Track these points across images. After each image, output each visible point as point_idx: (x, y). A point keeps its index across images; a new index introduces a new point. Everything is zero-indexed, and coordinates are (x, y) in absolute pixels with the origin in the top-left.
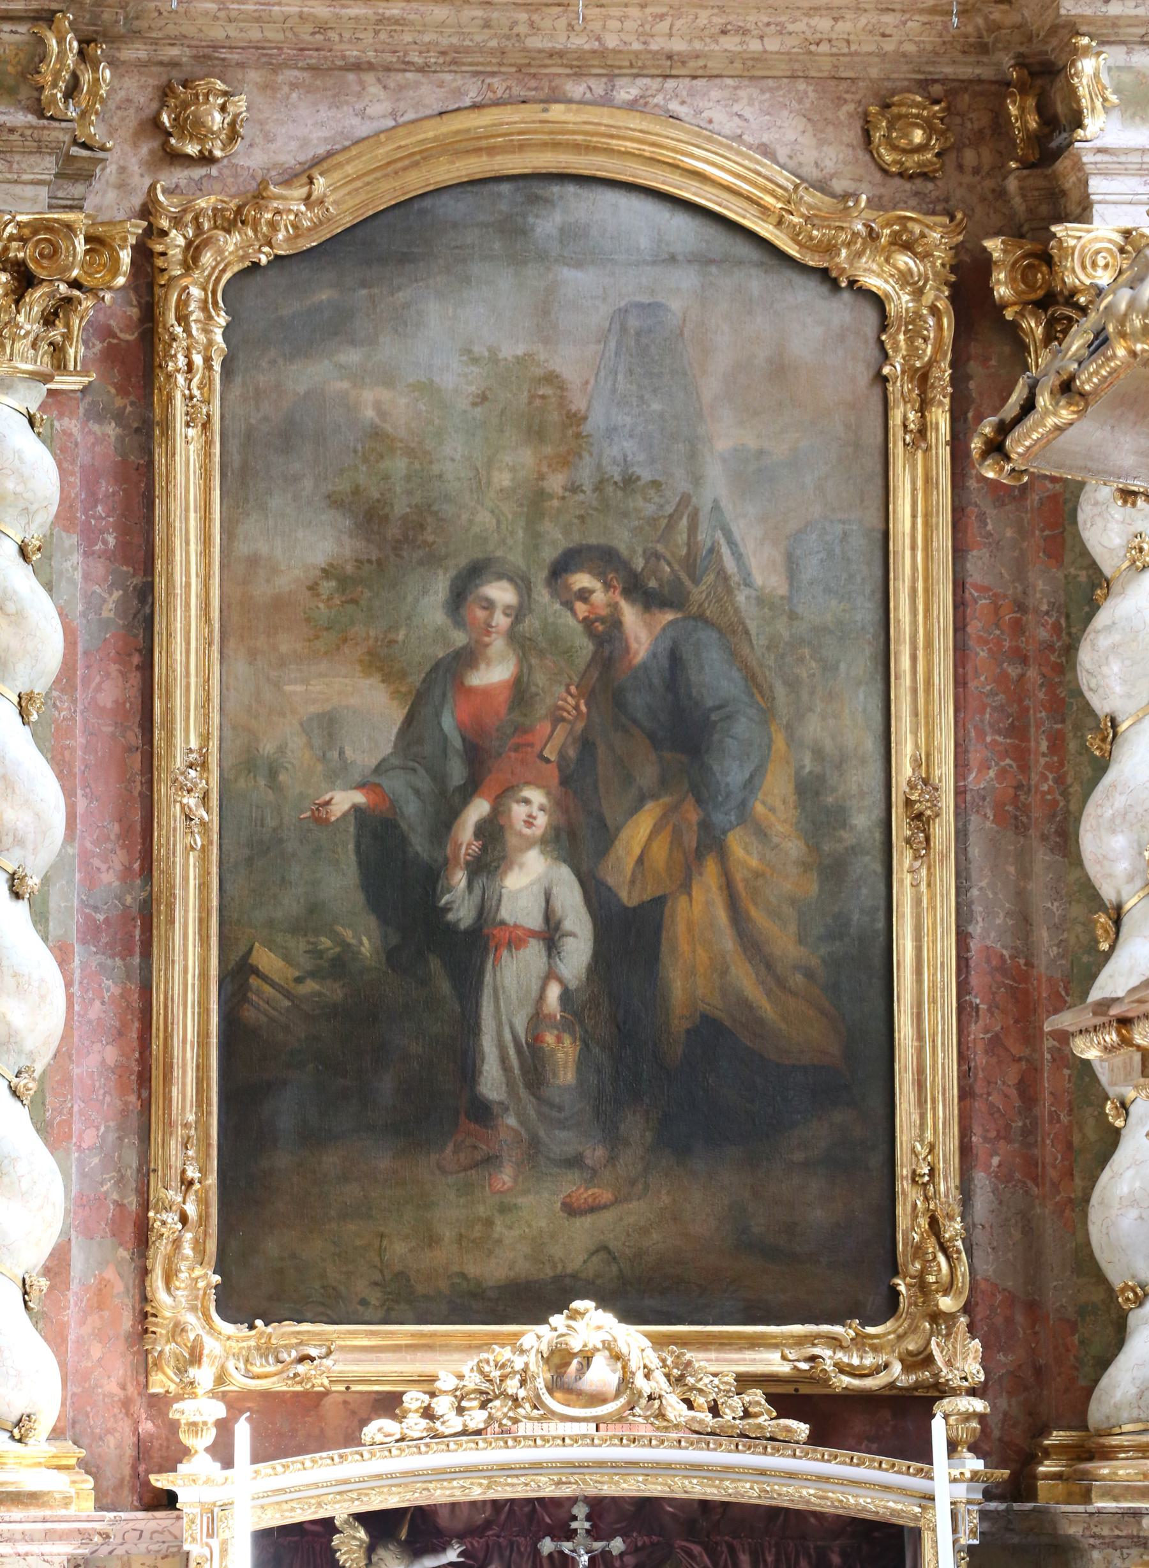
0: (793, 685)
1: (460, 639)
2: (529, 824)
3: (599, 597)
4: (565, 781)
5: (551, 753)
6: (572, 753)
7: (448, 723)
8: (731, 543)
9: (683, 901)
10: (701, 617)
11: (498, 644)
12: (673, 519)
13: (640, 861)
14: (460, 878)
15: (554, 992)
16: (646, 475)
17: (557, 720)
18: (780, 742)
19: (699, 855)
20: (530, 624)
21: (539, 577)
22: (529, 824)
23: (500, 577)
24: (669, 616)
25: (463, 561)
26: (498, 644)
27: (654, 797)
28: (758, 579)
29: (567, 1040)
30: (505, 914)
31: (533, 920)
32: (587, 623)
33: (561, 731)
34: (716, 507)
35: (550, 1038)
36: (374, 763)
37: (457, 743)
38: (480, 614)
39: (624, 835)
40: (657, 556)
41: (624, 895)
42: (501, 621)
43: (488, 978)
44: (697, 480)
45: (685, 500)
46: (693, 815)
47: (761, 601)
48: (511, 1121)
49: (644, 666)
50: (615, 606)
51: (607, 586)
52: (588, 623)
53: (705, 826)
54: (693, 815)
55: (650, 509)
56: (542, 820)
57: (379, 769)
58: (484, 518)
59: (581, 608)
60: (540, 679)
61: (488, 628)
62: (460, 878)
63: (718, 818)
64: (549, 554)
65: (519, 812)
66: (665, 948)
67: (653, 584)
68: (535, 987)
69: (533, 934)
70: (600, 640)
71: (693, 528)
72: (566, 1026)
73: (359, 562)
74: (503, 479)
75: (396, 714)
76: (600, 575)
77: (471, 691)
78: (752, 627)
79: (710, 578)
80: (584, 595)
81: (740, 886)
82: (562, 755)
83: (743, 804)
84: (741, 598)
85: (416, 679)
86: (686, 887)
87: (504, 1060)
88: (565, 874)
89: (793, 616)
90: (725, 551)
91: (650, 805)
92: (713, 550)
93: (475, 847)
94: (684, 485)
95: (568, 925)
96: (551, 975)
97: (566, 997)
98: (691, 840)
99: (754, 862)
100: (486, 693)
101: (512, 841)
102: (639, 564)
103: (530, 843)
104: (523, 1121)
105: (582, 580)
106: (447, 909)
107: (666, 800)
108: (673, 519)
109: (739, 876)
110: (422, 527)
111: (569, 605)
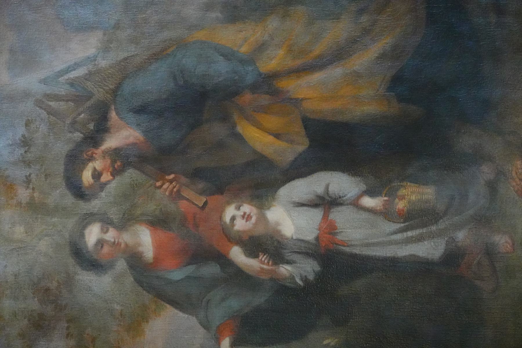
0: (162, 26)
1: (121, 265)
2: (247, 217)
3: (98, 164)
4: (220, 190)
5: (201, 200)
6: (201, 185)
7: (177, 275)
8: (67, 70)
9: (307, 105)
10: (115, 92)
11: (126, 238)
12: (51, 112)
13: (277, 136)
14: (285, 270)
15: (368, 202)
16: (21, 131)
17: (177, 196)
18: (200, 35)
19: (275, 93)
20: (114, 214)
21: (84, 207)
22: (247, 217)
23: (82, 235)
24: (113, 114)
25: (71, 261)
26: (126, 238)
27: (234, 126)
28: (92, 51)
29: (402, 192)
30: (310, 237)
31: (317, 215)
32: (115, 173)
33: (187, 193)
34: (44, 81)
35: (401, 205)
36: (202, 330)
37: (190, 269)
38: (106, 249)
39: (258, 147)
40: (74, 123)
41: (301, 148)
42: (111, 235)
43: (357, 251)
44: (26, 95)
45: (39, 103)
46: (248, 97)
47: (106, 49)
48: (461, 236)
49: (146, 132)
50: (105, 153)
51: (91, 159)
52: (115, 173)
53: (254, 88)
54: (248, 97)
55: (43, 128)
56: (246, 208)
57: (206, 326)
58: (44, 245)
59: (106, 177)
60: (151, 207)
61: (115, 244)
62: (285, 270)
63: (250, 79)
64: (69, 199)
65: (240, 225)
66: (340, 118)
67: (91, 126)
68: (365, 215)
69: (325, 217)
70: (126, 165)
71: (57, 98)
72: (392, 194)
73: (68, 336)
74: (19, 231)
75: (170, 311)
76: (84, 164)
77: (157, 259)
78: (123, 55)
79: (89, 85)
80: (97, 175)
81: (299, 62)
82: (202, 193)
83: (243, 62)
84: (103, 63)
85: (147, 297)
86: (297, 102)
87: (420, 239)
88: (284, 192)
89: (117, 26)
90: (73, 75)
91: (239, 129)
92: (72, 83)
93: (263, 257)
94: (29, 106)
95: (320, 190)
96: (355, 204)
97: (371, 193)
98: (264, 100)
99: (281, 52)
100: (158, 246)
101: (260, 230)
102: (78, 136)
103: (262, 218)
104: (459, 227)
105: (87, 176)
106: (305, 280)
107: (236, 117)
108: (51, 112)
109: (291, 63)
110: (47, 290)
111: (103, 186)
